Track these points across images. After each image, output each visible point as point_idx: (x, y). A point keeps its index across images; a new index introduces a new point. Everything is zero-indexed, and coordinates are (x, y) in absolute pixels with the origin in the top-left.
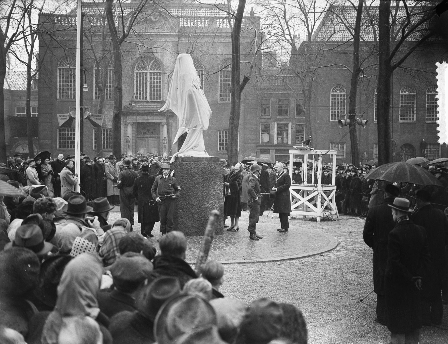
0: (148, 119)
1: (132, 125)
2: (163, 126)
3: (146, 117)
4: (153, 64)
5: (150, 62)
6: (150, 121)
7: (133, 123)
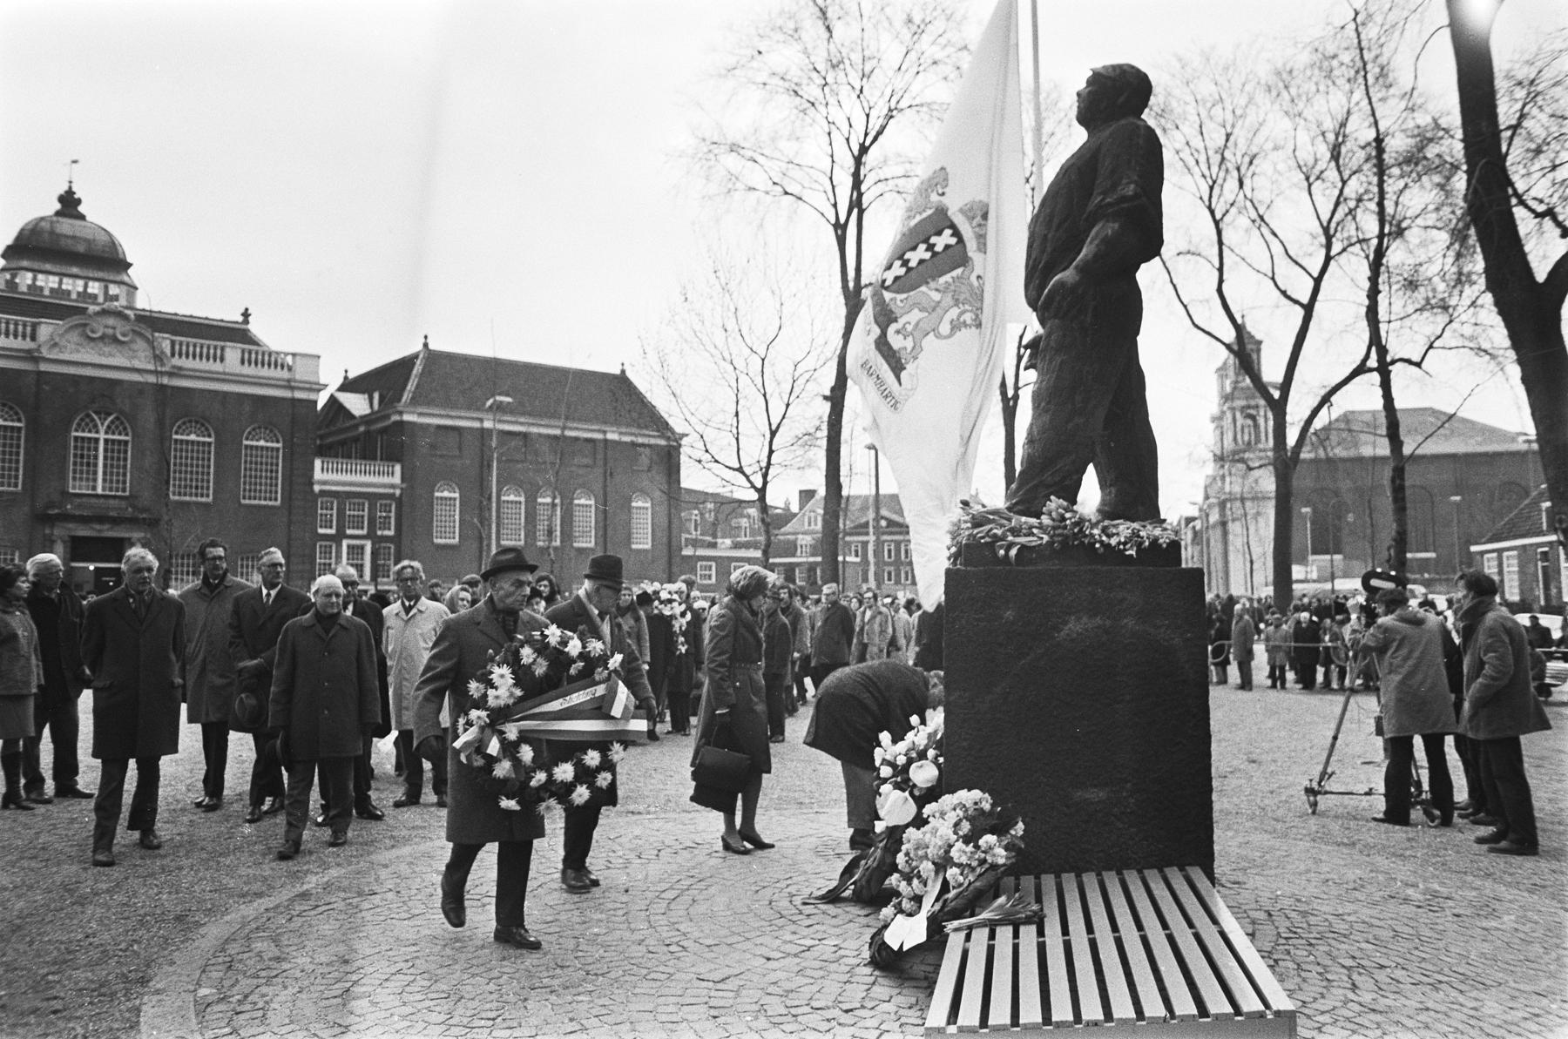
3: (98, 527)
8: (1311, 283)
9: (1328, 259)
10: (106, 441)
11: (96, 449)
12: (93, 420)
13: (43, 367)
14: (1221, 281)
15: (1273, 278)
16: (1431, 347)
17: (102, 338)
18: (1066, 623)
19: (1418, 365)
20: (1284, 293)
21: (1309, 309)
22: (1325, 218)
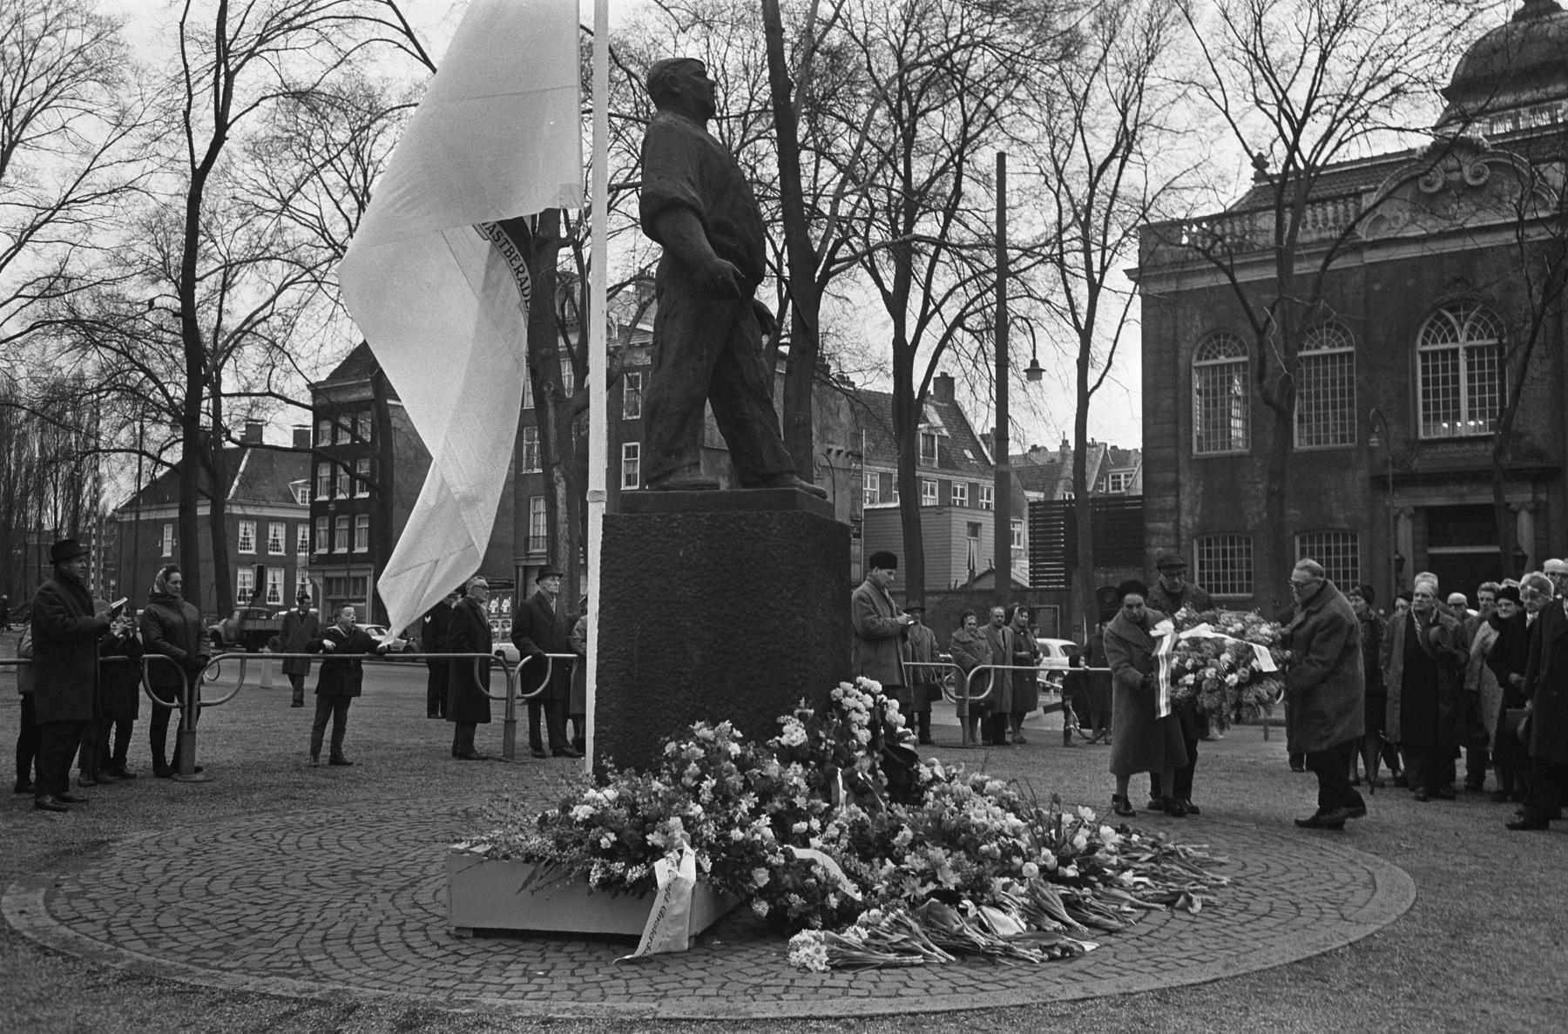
0: (1462, 495)
1: (1411, 517)
2: (1516, 514)
3: (1456, 489)
4: (1477, 320)
5: (1466, 317)
6: (1472, 500)
7: (1417, 508)
10: (1470, 350)
11: (1456, 368)
12: (1448, 322)
13: (1371, 257)
17: (1445, 189)
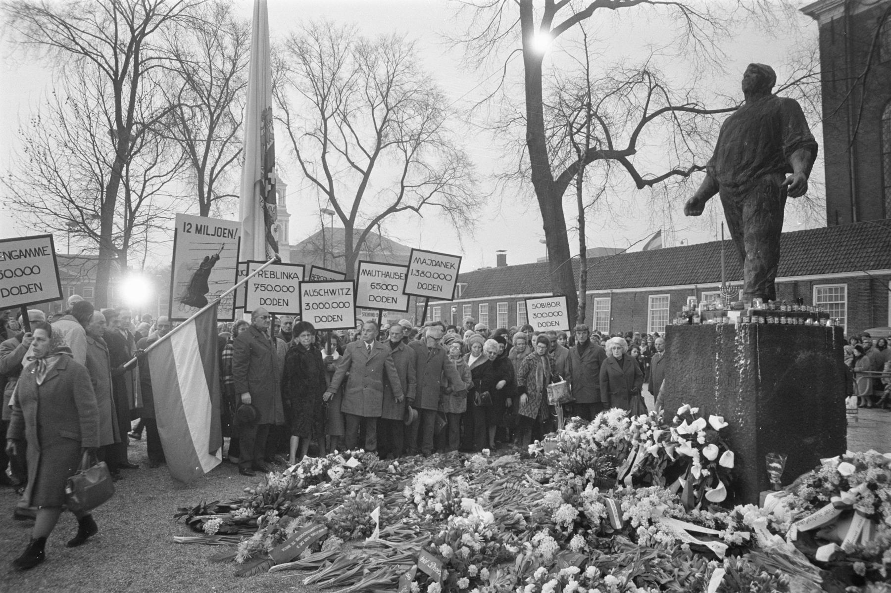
8: (369, 161)
9: (378, 149)
14: (324, 153)
15: (346, 155)
16: (423, 202)
18: (799, 354)
19: (417, 210)
20: (352, 164)
21: (367, 175)
22: (378, 127)
